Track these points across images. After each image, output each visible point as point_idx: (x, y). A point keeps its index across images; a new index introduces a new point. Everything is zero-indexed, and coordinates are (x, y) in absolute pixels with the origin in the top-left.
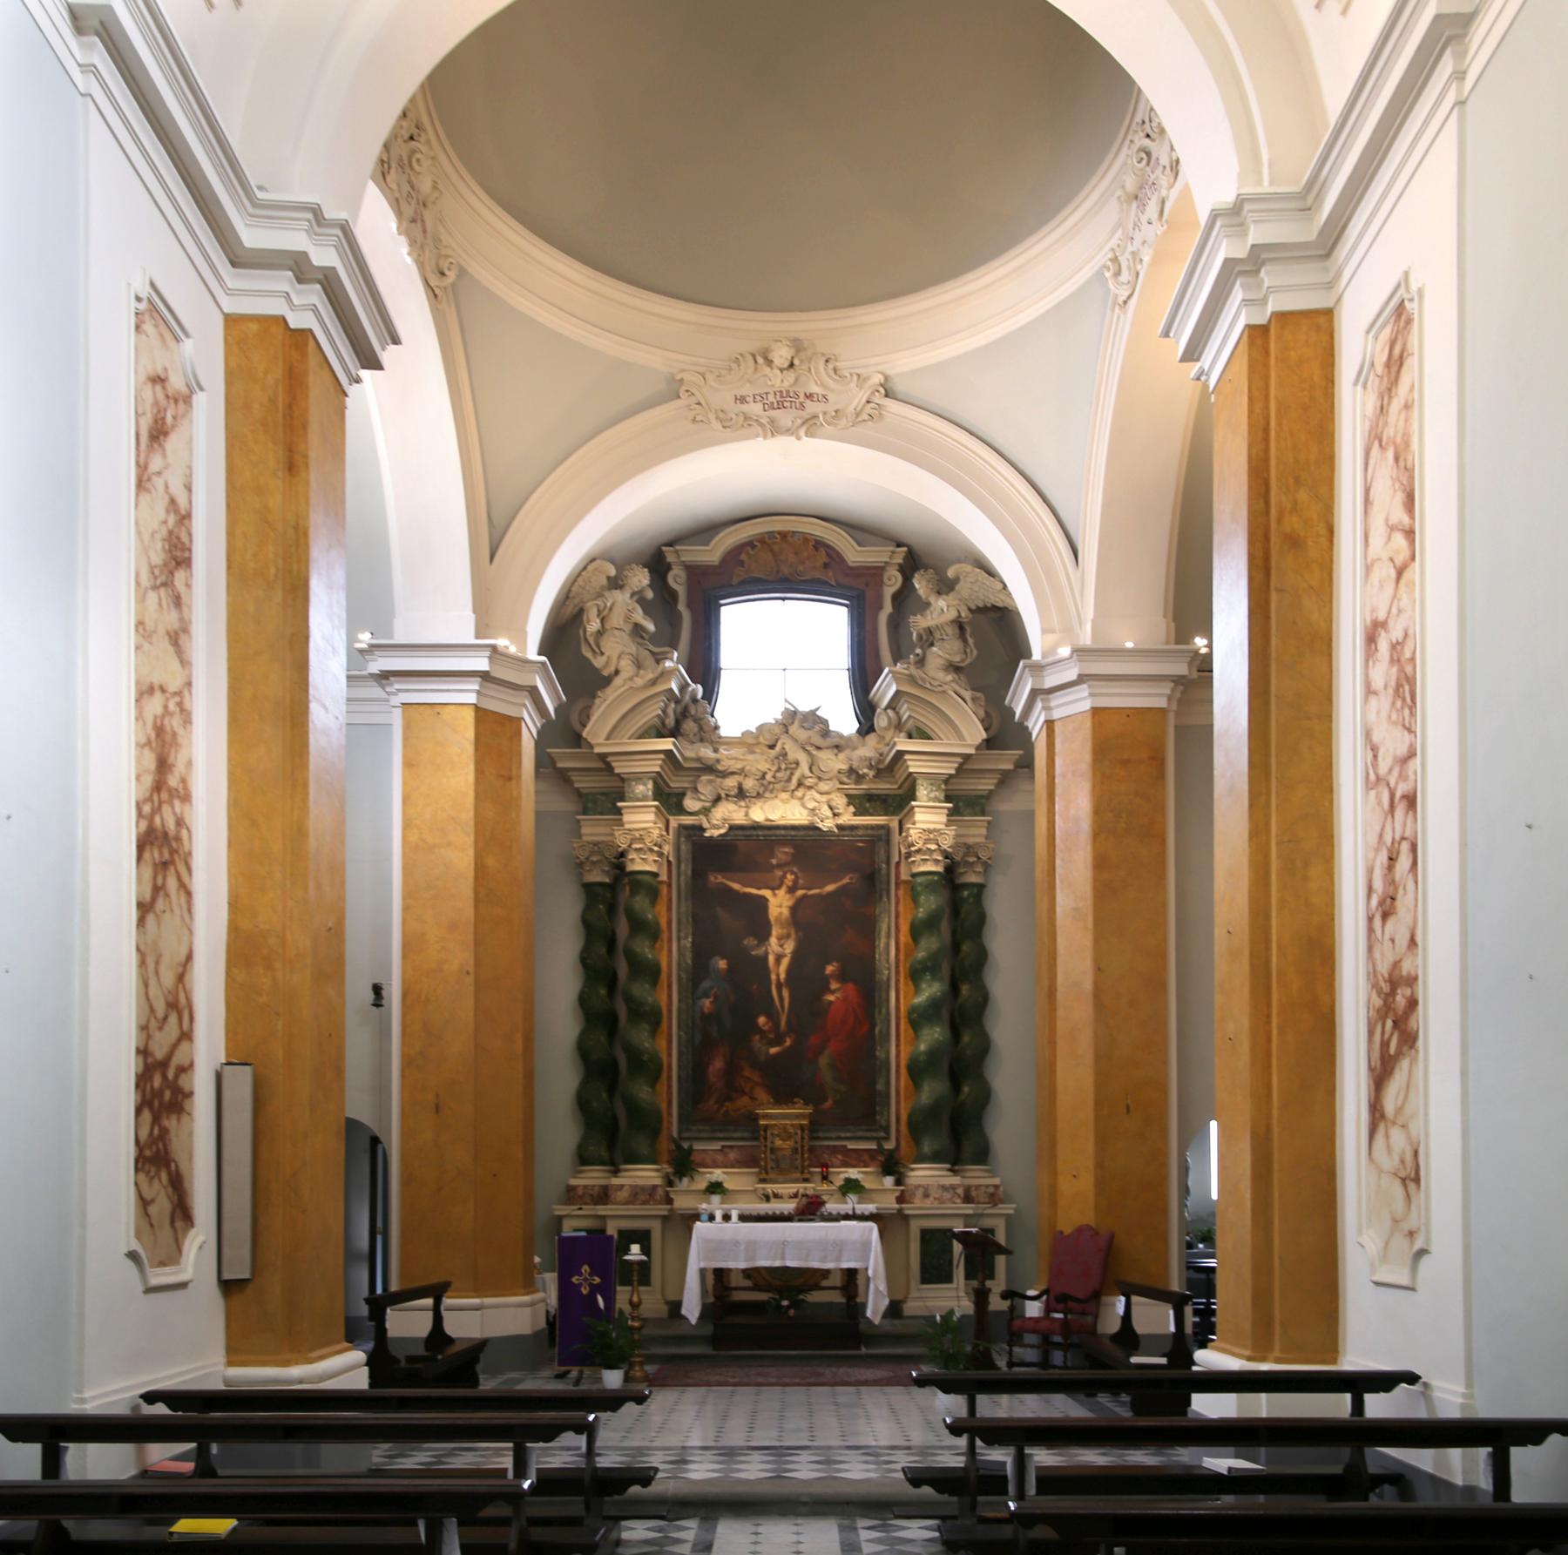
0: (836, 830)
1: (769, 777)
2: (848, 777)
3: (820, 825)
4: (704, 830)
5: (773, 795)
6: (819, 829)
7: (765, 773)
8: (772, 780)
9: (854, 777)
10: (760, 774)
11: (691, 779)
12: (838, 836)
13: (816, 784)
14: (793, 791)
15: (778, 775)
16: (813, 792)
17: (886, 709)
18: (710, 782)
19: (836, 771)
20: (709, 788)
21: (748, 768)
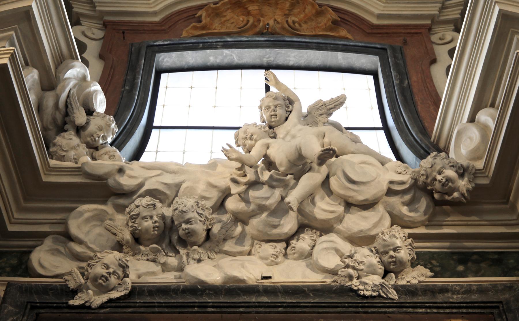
0: (394, 295)
1: (231, 204)
2: (408, 204)
3: (355, 284)
4: (74, 293)
5: (239, 249)
6: (356, 292)
7: (226, 194)
8: (241, 206)
9: (423, 203)
10: (214, 196)
11: (58, 216)
12: (400, 305)
13: (340, 220)
14: (288, 240)
15: (253, 194)
16: (333, 237)
17: (472, 119)
18: (100, 218)
19: (385, 187)
20: (98, 230)
21: (184, 186)
